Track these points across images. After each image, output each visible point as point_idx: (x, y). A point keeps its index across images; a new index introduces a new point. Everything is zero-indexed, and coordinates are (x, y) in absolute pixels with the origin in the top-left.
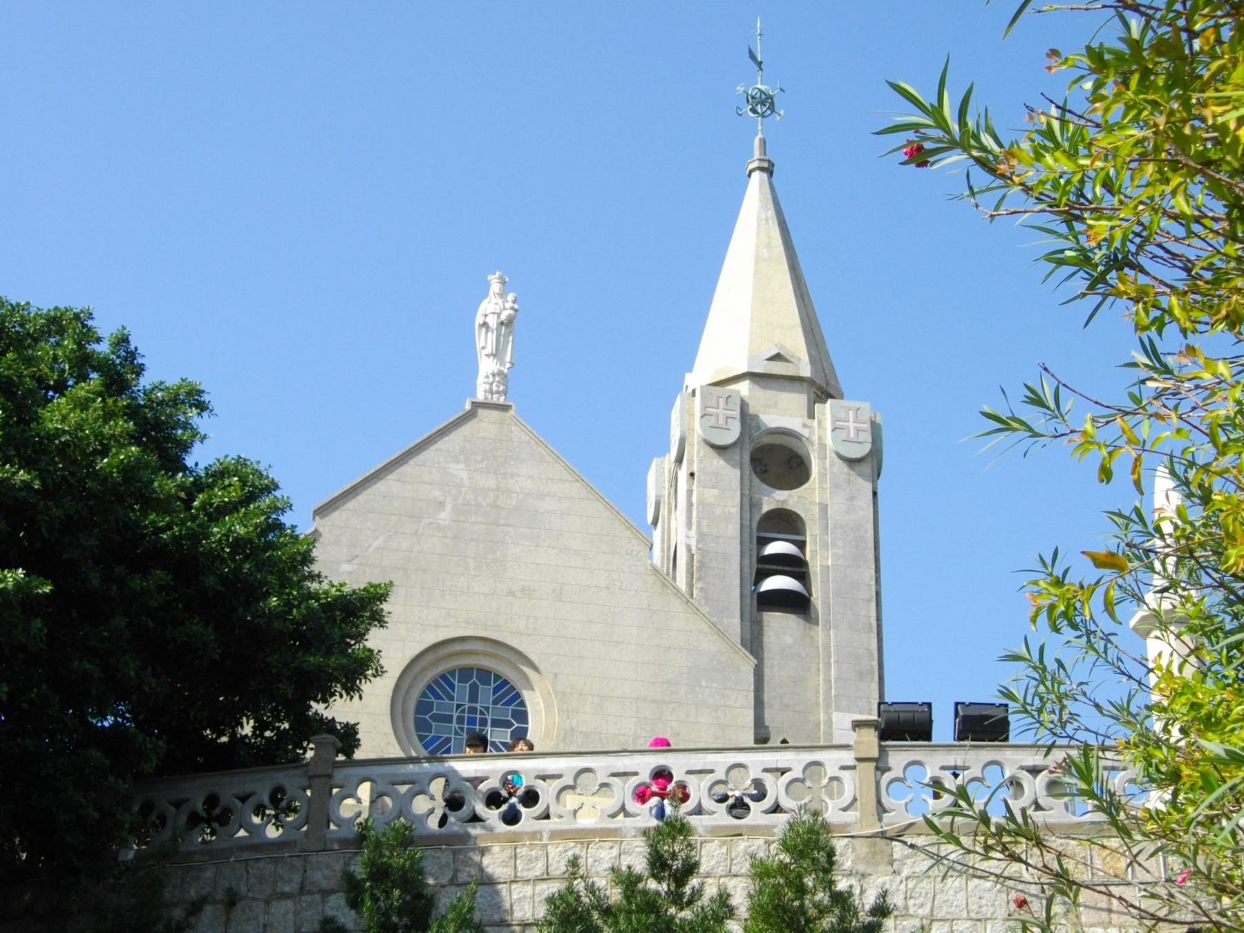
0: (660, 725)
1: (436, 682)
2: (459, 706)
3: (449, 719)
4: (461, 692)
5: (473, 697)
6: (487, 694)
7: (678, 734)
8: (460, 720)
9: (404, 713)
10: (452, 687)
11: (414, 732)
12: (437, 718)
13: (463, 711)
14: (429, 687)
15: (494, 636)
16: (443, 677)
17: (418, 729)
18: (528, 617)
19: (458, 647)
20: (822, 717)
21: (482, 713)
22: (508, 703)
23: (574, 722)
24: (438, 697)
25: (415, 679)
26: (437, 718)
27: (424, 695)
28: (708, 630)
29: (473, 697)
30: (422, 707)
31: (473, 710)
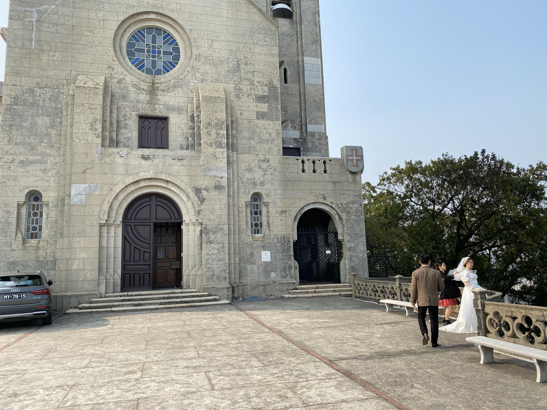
0: (239, 53)
1: (136, 33)
2: (147, 45)
3: (143, 51)
4: (148, 39)
5: (154, 41)
6: (160, 40)
7: (247, 58)
8: (148, 51)
9: (120, 47)
10: (144, 36)
11: (126, 56)
12: (137, 50)
13: (150, 47)
14: (133, 36)
15: (161, 11)
16: (139, 31)
17: (128, 55)
18: (177, 4)
19: (145, 16)
20: (300, 59)
21: (158, 48)
22: (170, 44)
23: (200, 51)
24: (137, 41)
25: (125, 31)
26: (137, 50)
27: (130, 39)
28: (257, 12)
29: (154, 41)
30: (130, 45)
31: (154, 47)
